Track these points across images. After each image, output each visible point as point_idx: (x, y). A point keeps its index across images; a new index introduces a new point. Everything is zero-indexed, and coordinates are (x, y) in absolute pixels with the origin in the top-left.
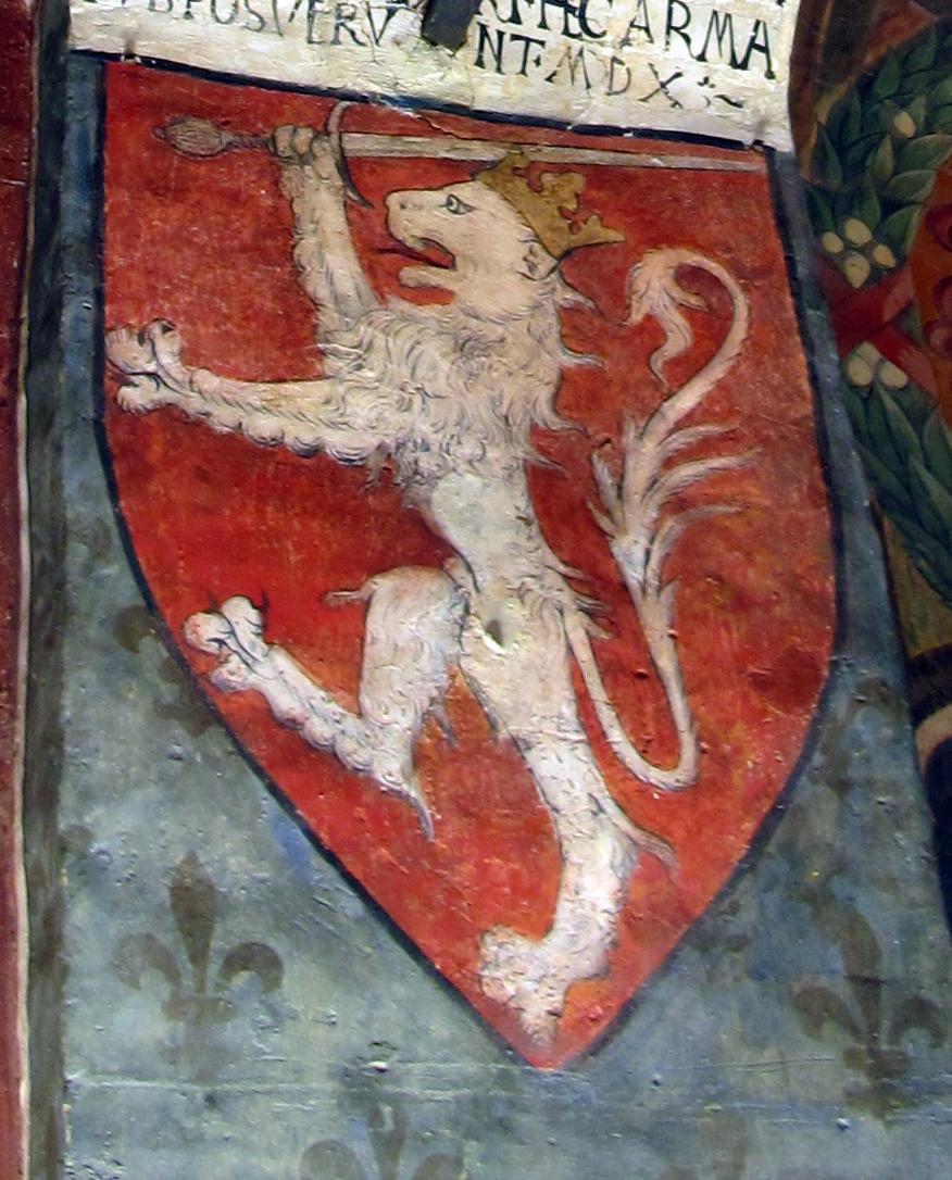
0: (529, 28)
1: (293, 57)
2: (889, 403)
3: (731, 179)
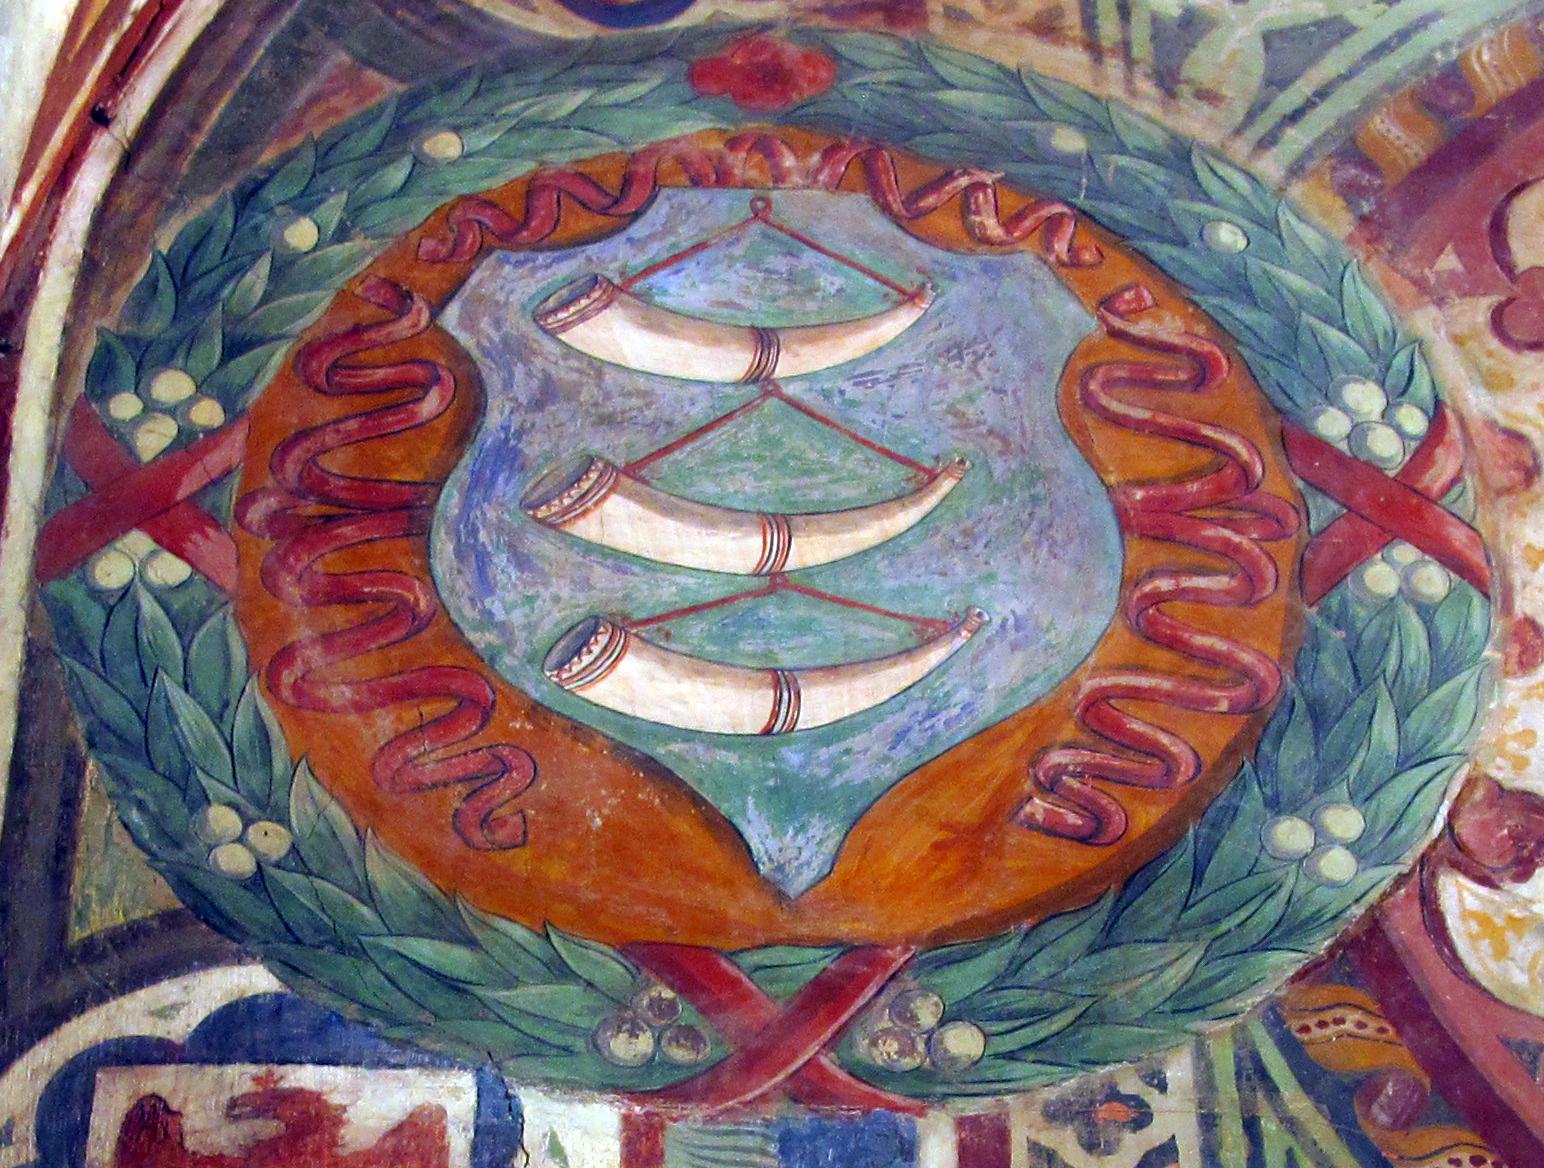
2: (149, 606)
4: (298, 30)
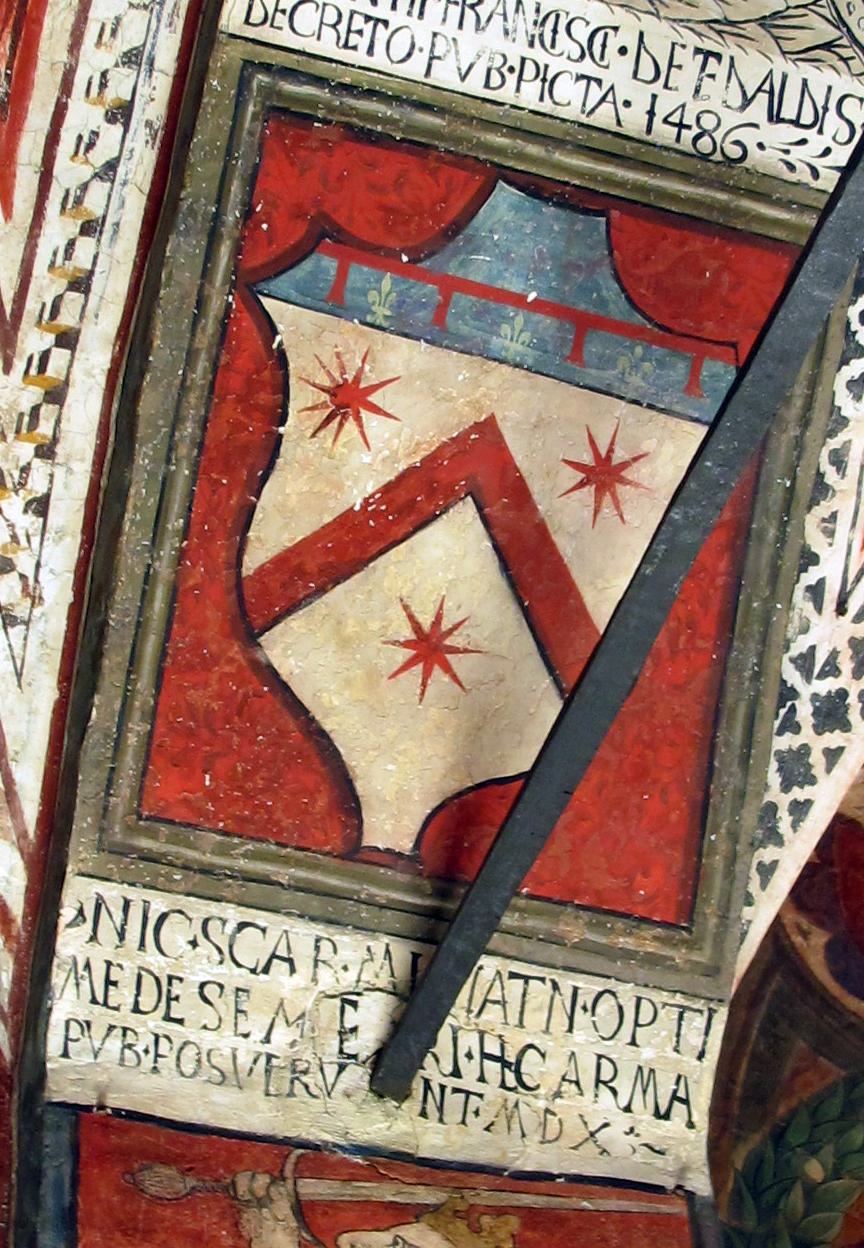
0: (469, 1081)
1: (252, 1108)
3: (655, 1221)
4: (771, 1020)
